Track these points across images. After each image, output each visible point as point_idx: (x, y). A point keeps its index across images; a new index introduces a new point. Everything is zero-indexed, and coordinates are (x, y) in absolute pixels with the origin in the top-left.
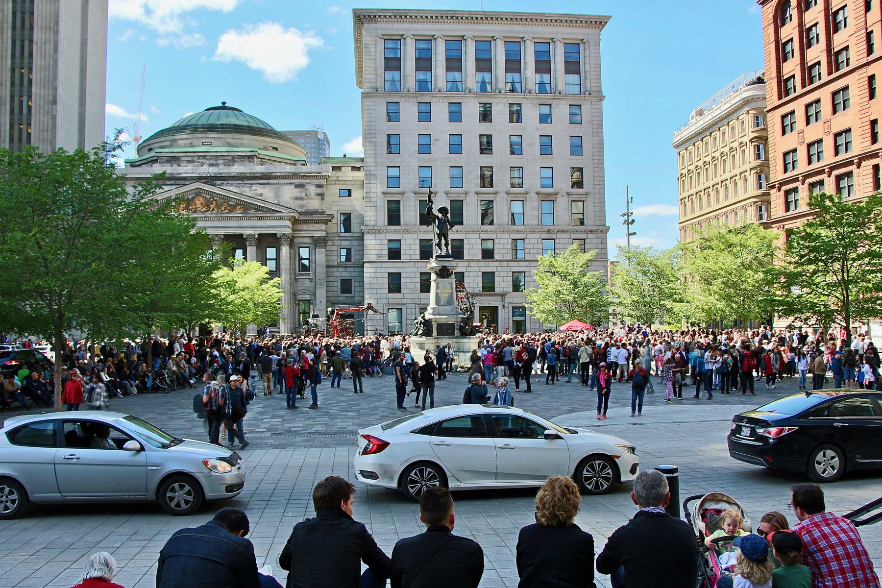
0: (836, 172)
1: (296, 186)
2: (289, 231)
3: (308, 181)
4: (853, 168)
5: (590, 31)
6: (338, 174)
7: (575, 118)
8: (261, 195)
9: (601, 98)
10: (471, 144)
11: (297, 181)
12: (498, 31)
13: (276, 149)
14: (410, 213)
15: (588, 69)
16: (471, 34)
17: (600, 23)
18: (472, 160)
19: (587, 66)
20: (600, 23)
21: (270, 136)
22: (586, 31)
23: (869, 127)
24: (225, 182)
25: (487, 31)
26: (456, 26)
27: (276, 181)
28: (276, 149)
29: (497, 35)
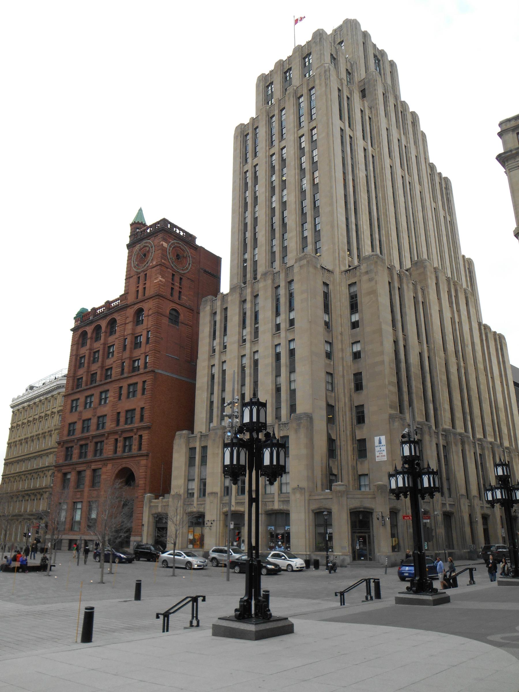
0: (95, 440)
4: (103, 439)
23: (116, 416)
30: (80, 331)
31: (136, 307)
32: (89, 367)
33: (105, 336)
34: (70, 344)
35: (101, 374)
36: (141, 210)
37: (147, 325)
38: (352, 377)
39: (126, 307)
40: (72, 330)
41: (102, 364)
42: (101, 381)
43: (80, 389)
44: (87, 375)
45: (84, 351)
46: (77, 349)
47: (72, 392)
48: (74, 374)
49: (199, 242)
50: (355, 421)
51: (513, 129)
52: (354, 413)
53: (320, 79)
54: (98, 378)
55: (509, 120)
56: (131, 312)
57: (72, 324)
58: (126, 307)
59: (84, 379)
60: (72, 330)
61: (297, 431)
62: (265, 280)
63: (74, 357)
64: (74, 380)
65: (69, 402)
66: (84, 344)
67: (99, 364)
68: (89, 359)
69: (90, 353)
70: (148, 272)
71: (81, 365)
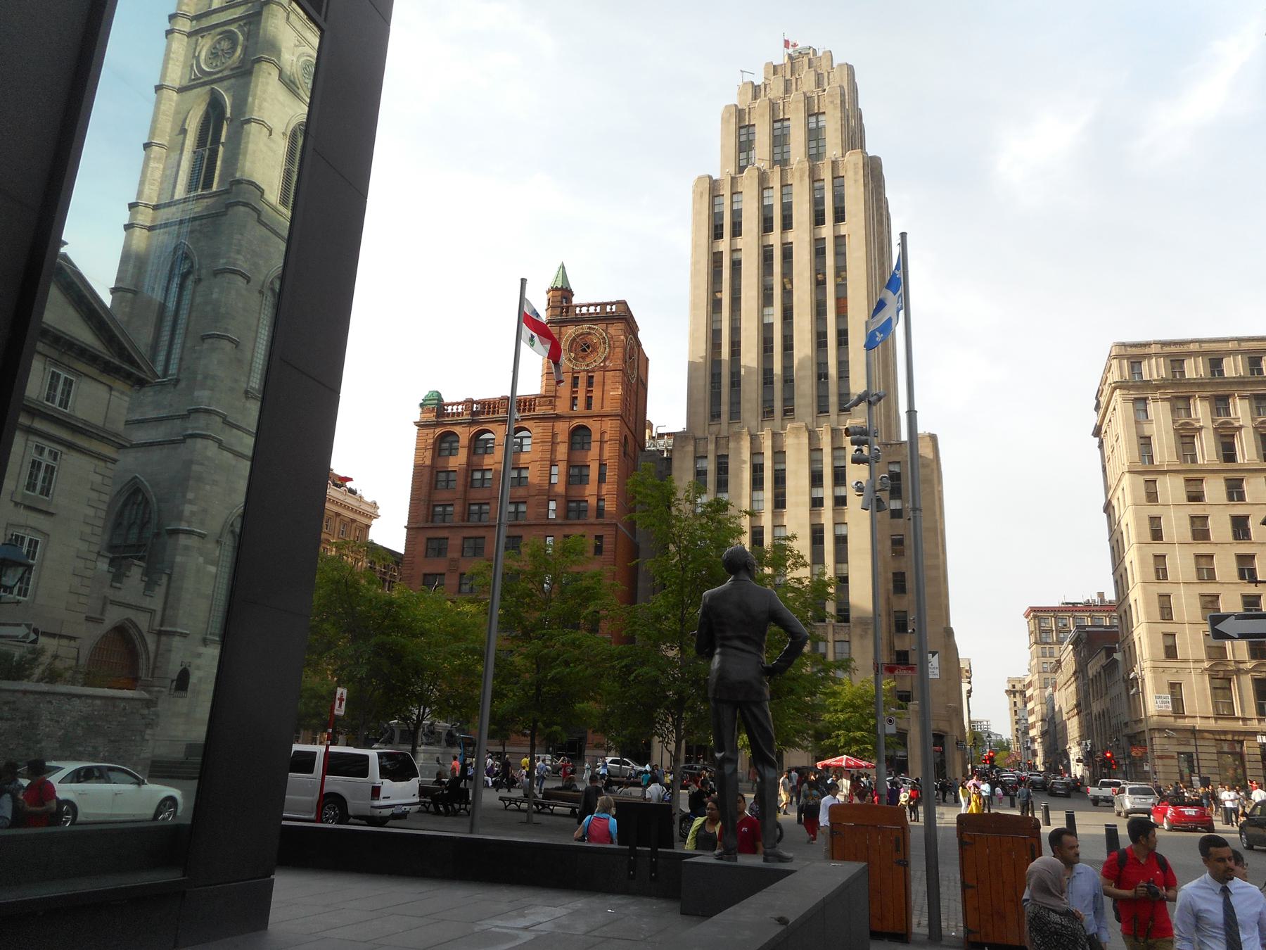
30: (439, 431)
31: (576, 422)
36: (563, 267)
37: (601, 455)
38: (890, 575)
39: (558, 417)
40: (417, 424)
49: (640, 335)
50: (893, 629)
51: (1129, 357)
52: (893, 620)
53: (856, 173)
55: (1124, 345)
56: (563, 428)
57: (416, 415)
58: (558, 417)
60: (417, 424)
61: (861, 637)
62: (797, 437)
65: (424, 541)
70: (597, 376)
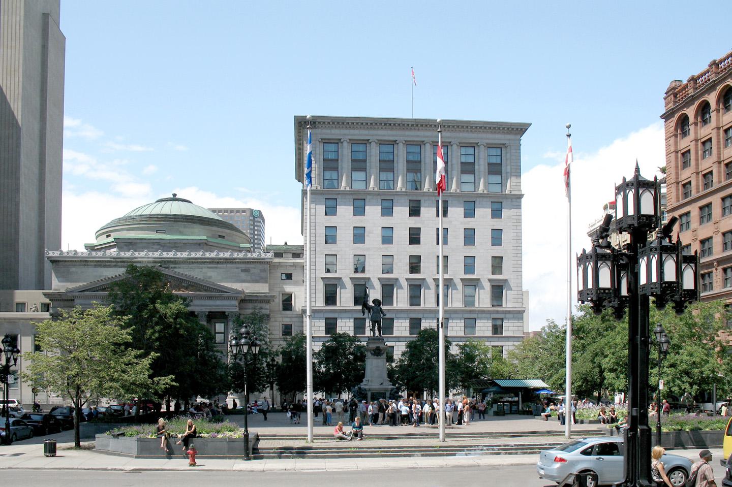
1: (242, 271)
2: (237, 309)
3: (252, 266)
5: (512, 137)
6: (281, 260)
7: (497, 213)
8: (210, 277)
9: (520, 197)
10: (401, 235)
11: (243, 266)
12: (427, 137)
13: (223, 237)
14: (345, 298)
15: (509, 170)
16: (403, 139)
17: (520, 129)
18: (402, 250)
19: (509, 167)
20: (520, 129)
21: (218, 226)
22: (508, 137)
24: (177, 266)
25: (418, 136)
26: (390, 132)
27: (224, 266)
28: (223, 237)
29: (425, 139)
32: (697, 165)
33: (718, 116)
34: (664, 138)
35: (719, 172)
41: (719, 157)
42: (720, 182)
43: (689, 199)
44: (697, 178)
45: (685, 143)
46: (676, 143)
47: (678, 204)
48: (677, 178)
54: (715, 178)
59: (693, 183)
63: (673, 155)
64: (677, 187)
66: (685, 134)
67: (714, 157)
68: (697, 153)
69: (696, 145)
71: (686, 164)
